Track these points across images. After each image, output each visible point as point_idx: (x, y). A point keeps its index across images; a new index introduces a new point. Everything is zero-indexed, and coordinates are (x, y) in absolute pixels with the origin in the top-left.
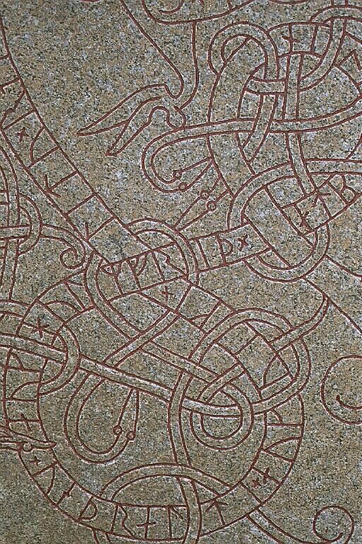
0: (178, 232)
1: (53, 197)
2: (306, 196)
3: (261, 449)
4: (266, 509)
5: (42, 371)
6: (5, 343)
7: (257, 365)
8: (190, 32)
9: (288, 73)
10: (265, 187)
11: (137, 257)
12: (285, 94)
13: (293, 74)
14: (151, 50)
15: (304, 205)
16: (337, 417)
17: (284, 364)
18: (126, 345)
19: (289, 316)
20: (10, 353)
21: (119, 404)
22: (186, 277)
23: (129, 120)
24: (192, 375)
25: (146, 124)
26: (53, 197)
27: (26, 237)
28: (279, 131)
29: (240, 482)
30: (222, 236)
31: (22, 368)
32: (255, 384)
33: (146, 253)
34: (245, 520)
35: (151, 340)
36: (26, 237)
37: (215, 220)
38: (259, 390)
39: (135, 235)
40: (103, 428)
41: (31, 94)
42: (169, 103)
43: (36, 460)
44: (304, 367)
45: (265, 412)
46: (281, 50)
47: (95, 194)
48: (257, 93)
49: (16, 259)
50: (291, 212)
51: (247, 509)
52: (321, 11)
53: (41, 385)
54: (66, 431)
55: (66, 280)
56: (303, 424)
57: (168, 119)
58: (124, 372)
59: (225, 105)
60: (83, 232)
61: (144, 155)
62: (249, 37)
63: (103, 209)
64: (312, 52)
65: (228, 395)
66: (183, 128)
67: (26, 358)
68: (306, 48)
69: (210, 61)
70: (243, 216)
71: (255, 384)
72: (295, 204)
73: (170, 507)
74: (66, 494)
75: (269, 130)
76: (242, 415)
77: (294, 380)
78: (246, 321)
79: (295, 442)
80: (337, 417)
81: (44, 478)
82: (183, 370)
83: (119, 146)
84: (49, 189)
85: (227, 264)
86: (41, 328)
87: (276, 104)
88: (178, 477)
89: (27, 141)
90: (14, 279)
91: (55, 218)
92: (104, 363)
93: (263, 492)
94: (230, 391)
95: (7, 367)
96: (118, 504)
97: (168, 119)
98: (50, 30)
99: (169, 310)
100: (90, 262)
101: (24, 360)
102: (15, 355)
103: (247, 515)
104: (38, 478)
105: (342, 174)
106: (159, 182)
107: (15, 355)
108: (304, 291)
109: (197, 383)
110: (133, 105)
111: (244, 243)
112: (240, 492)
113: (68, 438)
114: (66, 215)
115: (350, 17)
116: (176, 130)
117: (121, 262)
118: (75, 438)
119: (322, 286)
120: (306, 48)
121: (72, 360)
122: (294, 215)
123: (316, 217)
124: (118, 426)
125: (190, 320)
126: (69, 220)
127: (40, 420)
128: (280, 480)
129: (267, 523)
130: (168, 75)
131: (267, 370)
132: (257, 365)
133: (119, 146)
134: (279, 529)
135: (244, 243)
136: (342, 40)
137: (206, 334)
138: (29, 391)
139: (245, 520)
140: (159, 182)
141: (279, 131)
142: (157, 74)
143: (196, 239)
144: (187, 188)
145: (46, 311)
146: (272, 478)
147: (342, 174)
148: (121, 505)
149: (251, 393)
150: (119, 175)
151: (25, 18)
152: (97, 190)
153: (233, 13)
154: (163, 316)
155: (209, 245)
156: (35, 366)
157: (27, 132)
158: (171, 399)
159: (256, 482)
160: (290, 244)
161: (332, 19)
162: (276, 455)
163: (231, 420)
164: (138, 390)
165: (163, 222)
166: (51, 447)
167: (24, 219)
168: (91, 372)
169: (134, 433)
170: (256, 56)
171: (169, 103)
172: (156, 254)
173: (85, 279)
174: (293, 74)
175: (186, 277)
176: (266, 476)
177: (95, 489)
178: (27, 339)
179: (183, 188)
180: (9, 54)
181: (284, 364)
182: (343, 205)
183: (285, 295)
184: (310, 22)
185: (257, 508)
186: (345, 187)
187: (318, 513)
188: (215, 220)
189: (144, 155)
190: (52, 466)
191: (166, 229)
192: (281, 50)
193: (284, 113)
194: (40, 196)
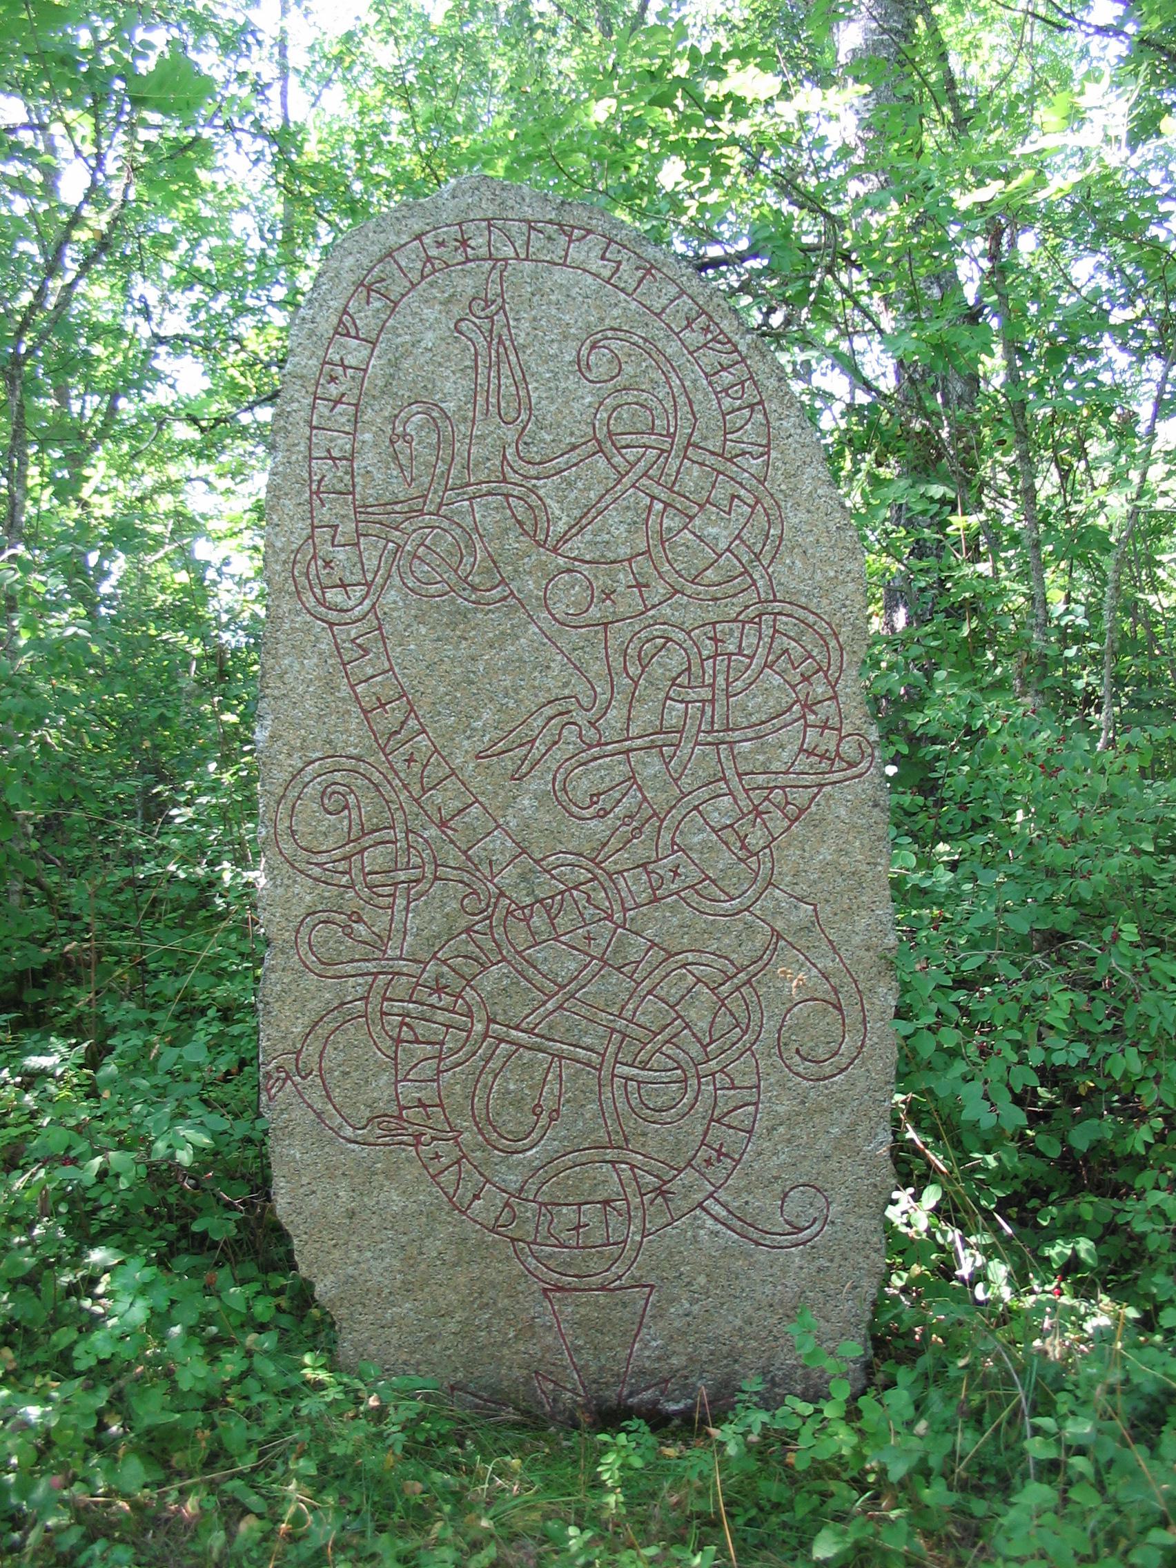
0: (598, 865)
1: (450, 832)
2: (744, 815)
3: (712, 1120)
4: (722, 1195)
5: (442, 1043)
6: (395, 1010)
7: (699, 1017)
8: (601, 636)
9: (715, 677)
10: (696, 808)
11: (552, 897)
12: (713, 701)
13: (721, 680)
14: (559, 657)
15: (743, 827)
16: (798, 1074)
17: (732, 1014)
18: (545, 1003)
19: (733, 956)
20: (403, 1024)
21: (538, 1076)
22: (610, 918)
23: (534, 740)
24: (625, 1035)
25: (556, 743)
26: (450, 832)
27: (417, 881)
28: (709, 744)
29: (689, 1164)
30: (651, 867)
31: (417, 1041)
32: (699, 1041)
33: (562, 893)
34: (698, 1212)
35: (572, 996)
36: (417, 881)
37: (641, 849)
38: (705, 1047)
39: (548, 872)
40: (520, 1109)
41: (420, 713)
42: (580, 717)
43: (438, 1157)
44: (755, 1017)
45: (713, 1074)
46: (705, 653)
47: (498, 826)
48: (681, 702)
49: (407, 909)
50: (725, 834)
51: (699, 1197)
52: (747, 607)
53: (441, 1060)
54: (474, 1116)
55: (468, 930)
56: (758, 1087)
57: (580, 736)
58: (542, 1037)
59: (644, 717)
60: (487, 872)
61: (554, 779)
62: (669, 639)
63: (509, 843)
64: (740, 653)
65: (668, 1057)
66: (599, 745)
67: (421, 1028)
68: (732, 648)
69: (625, 668)
70: (674, 843)
71: (699, 1041)
72: (731, 826)
73: (606, 1202)
74: (476, 1197)
75: (697, 744)
76: (686, 1080)
77: (745, 1033)
78: (684, 966)
79: (751, 1108)
80: (798, 1074)
81: (448, 1177)
82: (613, 1030)
83: (524, 769)
84: (443, 824)
85: (657, 900)
86: (439, 990)
87: (703, 712)
88: (613, 1162)
89: (416, 767)
90: (405, 933)
91: (453, 856)
92: (517, 1028)
93: (718, 1173)
94: (670, 1052)
95: (398, 1041)
96: (541, 1204)
97: (580, 736)
98: (439, 639)
99: (594, 958)
100: (496, 904)
101: (419, 1031)
102: (408, 1025)
103: (700, 1205)
104: (442, 1178)
105: (782, 788)
106: (574, 809)
107: (408, 1025)
108: (749, 926)
109: (630, 1044)
110: (540, 722)
111: (676, 874)
112: (689, 1176)
113: (477, 1124)
114: (465, 853)
115: (780, 613)
116: (590, 746)
117: (532, 905)
118: (487, 1123)
119: (769, 919)
120: (732, 648)
121: (479, 1027)
122: (733, 839)
123: (756, 839)
124: (538, 1105)
125: (618, 969)
126: (469, 858)
127: (441, 1105)
128: (737, 1157)
129: (725, 1213)
130: (580, 688)
131: (712, 1023)
132: (699, 1017)
133: (524, 769)
134: (739, 1219)
135: (676, 874)
136: (772, 638)
137: (639, 984)
138: (429, 1068)
139: (698, 1212)
140: (574, 809)
141: (709, 744)
142: (566, 685)
143: (620, 872)
144: (607, 813)
145: (445, 969)
146: (726, 1155)
147: (782, 788)
148: (545, 1205)
149: (695, 1050)
150: (526, 802)
151: (409, 626)
152: (501, 821)
153: (651, 613)
154: (586, 966)
155: (637, 880)
156: (433, 1038)
157: (416, 756)
158: (601, 1064)
159: (708, 1162)
160: (730, 872)
161: (760, 616)
162: (730, 1127)
163: (674, 1086)
164: (561, 1058)
165: (581, 855)
166: (455, 1138)
167: (415, 860)
168: (502, 1041)
169: (557, 1111)
170: (675, 660)
171: (580, 717)
172: (575, 893)
173: (491, 927)
174: (721, 680)
175: (610, 918)
176: (718, 1151)
177: (513, 1187)
178: (422, 1004)
179: (602, 814)
180: (391, 669)
181: (732, 1014)
182: (786, 823)
183: (728, 932)
184: (735, 620)
185: (711, 1195)
186: (788, 803)
187: (786, 1195)
188: (641, 849)
189: (554, 779)
190: (458, 1162)
191: (584, 862)
192: (705, 653)
193: (713, 723)
194: (432, 832)
